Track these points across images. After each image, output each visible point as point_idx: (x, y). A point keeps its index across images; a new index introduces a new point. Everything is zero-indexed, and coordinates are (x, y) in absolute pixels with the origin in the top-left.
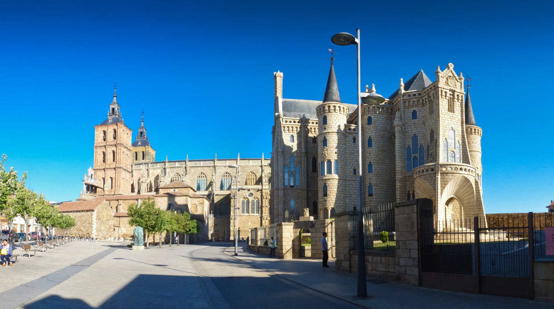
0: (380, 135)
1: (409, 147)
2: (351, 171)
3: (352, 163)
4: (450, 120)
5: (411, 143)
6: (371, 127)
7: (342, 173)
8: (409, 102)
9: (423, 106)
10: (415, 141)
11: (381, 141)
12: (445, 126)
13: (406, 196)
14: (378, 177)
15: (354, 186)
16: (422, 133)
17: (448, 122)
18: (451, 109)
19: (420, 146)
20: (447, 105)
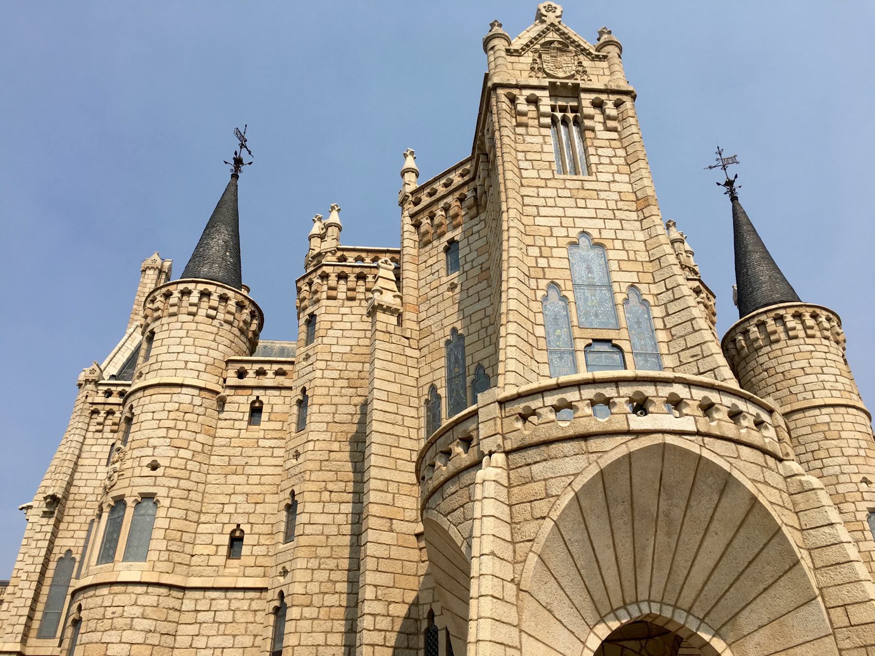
0: (346, 374)
1: (433, 388)
2: (217, 546)
3: (229, 509)
4: (571, 202)
5: (443, 373)
6: (311, 353)
7: (165, 555)
8: (432, 217)
9: (478, 214)
10: (456, 358)
11: (345, 400)
12: (545, 231)
13: (421, 649)
14: (316, 557)
15: (220, 617)
16: (480, 315)
17: (560, 212)
19: (476, 373)
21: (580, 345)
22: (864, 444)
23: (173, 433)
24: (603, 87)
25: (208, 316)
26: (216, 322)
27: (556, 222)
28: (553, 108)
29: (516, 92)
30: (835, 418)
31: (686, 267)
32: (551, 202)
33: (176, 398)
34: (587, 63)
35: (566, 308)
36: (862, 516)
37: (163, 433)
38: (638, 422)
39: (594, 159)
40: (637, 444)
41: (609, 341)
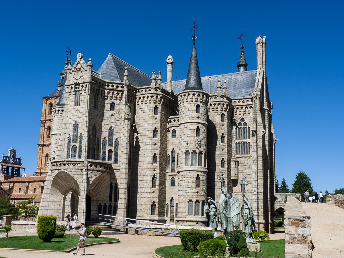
18: (77, 103)
20: (74, 100)
21: (71, 147)
22: (191, 133)
23: (56, 145)
24: (83, 82)
25: (60, 116)
26: (62, 117)
27: (71, 120)
28: (76, 88)
29: (69, 86)
30: (186, 126)
31: (152, 88)
32: (72, 115)
33: (56, 137)
34: (83, 72)
35: (71, 139)
36: (184, 152)
37: (55, 145)
38: (59, 167)
39: (81, 102)
40: (60, 171)
41: (75, 146)
